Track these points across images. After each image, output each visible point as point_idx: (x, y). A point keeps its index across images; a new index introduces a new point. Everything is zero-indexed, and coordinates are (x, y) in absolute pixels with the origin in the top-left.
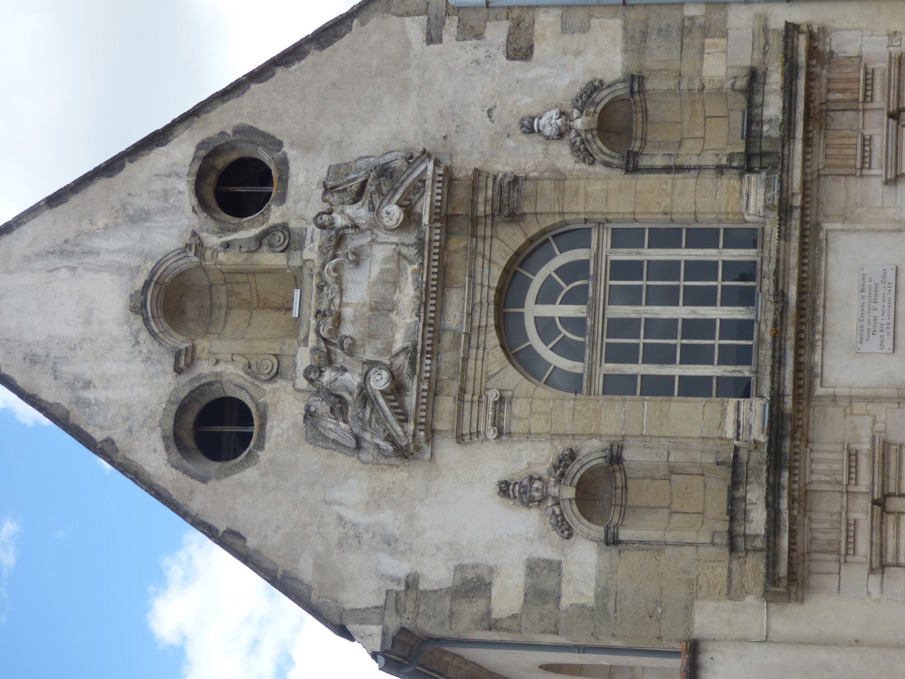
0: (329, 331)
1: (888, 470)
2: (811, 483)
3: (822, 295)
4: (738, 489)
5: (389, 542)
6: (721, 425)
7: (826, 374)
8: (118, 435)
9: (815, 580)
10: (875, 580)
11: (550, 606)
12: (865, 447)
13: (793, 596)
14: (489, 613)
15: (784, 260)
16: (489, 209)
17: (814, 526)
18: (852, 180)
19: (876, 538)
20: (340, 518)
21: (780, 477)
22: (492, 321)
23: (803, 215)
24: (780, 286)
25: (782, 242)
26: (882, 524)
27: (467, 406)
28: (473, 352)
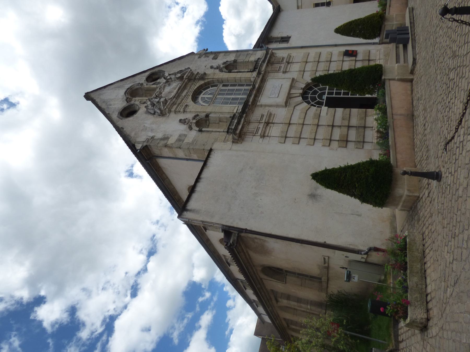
0: (158, 94)
1: (271, 118)
2: (251, 120)
3: (264, 88)
4: (233, 120)
5: (152, 130)
6: (233, 110)
7: (260, 101)
8: (111, 113)
9: (246, 139)
10: (262, 139)
11: (181, 142)
12: (266, 114)
13: (239, 140)
14: (167, 143)
15: (257, 80)
16: (198, 78)
17: (249, 128)
18: (276, 73)
19: (264, 129)
20: (144, 126)
21: (243, 115)
22: (191, 94)
23: (263, 77)
24: (254, 84)
25: (257, 77)
26: (266, 127)
27: (179, 106)
28: (185, 99)
